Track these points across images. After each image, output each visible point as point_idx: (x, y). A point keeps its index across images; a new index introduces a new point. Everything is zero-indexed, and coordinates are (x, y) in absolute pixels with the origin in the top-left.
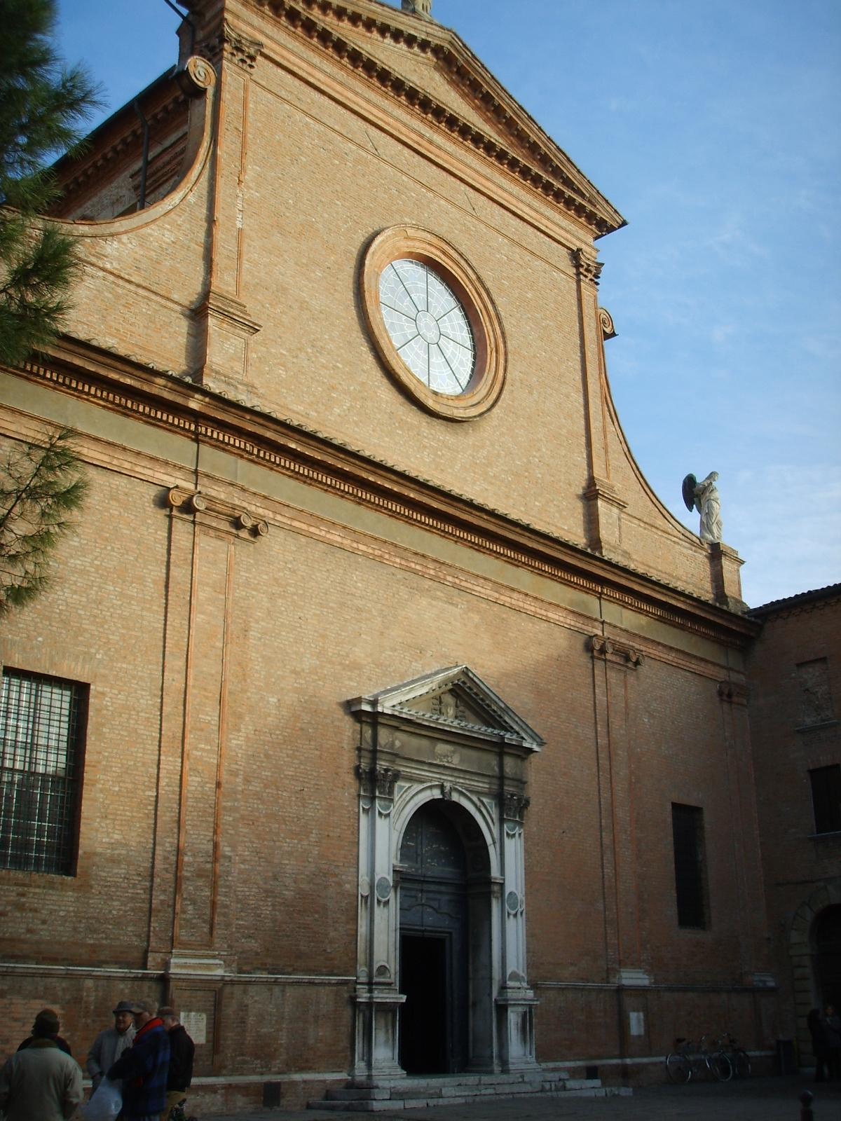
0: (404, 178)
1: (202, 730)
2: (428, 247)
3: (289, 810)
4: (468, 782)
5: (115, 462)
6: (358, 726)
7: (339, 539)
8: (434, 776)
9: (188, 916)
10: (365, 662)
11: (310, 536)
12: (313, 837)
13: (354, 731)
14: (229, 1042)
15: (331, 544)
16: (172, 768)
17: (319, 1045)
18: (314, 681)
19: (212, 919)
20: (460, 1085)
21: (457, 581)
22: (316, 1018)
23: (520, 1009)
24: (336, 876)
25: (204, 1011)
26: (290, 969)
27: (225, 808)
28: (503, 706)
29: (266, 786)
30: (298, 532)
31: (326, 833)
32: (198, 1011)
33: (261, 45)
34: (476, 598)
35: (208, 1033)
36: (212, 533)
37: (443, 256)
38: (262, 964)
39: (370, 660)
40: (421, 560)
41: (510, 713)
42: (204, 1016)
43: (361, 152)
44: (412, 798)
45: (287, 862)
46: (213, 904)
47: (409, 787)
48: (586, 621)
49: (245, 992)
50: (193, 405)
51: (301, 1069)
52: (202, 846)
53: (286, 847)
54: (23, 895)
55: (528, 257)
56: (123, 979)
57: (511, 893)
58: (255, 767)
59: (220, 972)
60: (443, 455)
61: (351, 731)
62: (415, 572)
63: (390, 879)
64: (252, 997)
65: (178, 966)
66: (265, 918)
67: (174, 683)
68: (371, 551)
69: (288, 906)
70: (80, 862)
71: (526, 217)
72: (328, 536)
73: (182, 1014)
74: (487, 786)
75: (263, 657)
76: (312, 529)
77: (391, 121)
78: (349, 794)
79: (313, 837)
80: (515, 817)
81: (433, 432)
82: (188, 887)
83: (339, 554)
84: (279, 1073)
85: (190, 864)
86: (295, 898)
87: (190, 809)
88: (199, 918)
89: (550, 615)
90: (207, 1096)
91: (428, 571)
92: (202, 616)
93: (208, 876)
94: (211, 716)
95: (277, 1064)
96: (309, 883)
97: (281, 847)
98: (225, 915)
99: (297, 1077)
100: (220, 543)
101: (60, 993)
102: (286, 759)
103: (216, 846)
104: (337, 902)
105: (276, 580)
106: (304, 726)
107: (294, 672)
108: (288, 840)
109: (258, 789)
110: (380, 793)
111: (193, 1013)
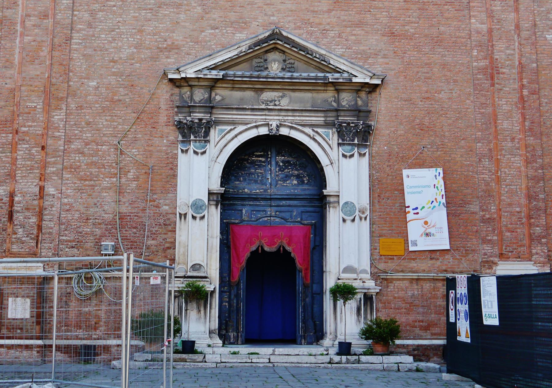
1: (30, 113)
4: (298, 118)
8: (259, 118)
9: (18, 236)
10: (185, 43)
12: (130, 175)
13: (172, 95)
16: (5, 141)
19: (38, 236)
25: (28, 297)
27: (49, 162)
29: (87, 144)
32: (23, 297)
42: (28, 301)
44: (236, 136)
46: (40, 228)
47: (231, 130)
52: (30, 190)
53: (105, 184)
57: (346, 203)
58: (76, 132)
67: (6, 86)
69: (107, 225)
73: (10, 299)
74: (323, 119)
75: (84, 55)
79: (130, 175)
80: (353, 140)
82: (19, 217)
85: (19, 203)
87: (19, 166)
88: (27, 237)
92: (29, 38)
94: (36, 103)
97: (101, 184)
102: (104, 123)
103: (42, 189)
106: (121, 98)
108: (107, 179)
109: (80, 147)
110: (195, 137)
111: (19, 299)
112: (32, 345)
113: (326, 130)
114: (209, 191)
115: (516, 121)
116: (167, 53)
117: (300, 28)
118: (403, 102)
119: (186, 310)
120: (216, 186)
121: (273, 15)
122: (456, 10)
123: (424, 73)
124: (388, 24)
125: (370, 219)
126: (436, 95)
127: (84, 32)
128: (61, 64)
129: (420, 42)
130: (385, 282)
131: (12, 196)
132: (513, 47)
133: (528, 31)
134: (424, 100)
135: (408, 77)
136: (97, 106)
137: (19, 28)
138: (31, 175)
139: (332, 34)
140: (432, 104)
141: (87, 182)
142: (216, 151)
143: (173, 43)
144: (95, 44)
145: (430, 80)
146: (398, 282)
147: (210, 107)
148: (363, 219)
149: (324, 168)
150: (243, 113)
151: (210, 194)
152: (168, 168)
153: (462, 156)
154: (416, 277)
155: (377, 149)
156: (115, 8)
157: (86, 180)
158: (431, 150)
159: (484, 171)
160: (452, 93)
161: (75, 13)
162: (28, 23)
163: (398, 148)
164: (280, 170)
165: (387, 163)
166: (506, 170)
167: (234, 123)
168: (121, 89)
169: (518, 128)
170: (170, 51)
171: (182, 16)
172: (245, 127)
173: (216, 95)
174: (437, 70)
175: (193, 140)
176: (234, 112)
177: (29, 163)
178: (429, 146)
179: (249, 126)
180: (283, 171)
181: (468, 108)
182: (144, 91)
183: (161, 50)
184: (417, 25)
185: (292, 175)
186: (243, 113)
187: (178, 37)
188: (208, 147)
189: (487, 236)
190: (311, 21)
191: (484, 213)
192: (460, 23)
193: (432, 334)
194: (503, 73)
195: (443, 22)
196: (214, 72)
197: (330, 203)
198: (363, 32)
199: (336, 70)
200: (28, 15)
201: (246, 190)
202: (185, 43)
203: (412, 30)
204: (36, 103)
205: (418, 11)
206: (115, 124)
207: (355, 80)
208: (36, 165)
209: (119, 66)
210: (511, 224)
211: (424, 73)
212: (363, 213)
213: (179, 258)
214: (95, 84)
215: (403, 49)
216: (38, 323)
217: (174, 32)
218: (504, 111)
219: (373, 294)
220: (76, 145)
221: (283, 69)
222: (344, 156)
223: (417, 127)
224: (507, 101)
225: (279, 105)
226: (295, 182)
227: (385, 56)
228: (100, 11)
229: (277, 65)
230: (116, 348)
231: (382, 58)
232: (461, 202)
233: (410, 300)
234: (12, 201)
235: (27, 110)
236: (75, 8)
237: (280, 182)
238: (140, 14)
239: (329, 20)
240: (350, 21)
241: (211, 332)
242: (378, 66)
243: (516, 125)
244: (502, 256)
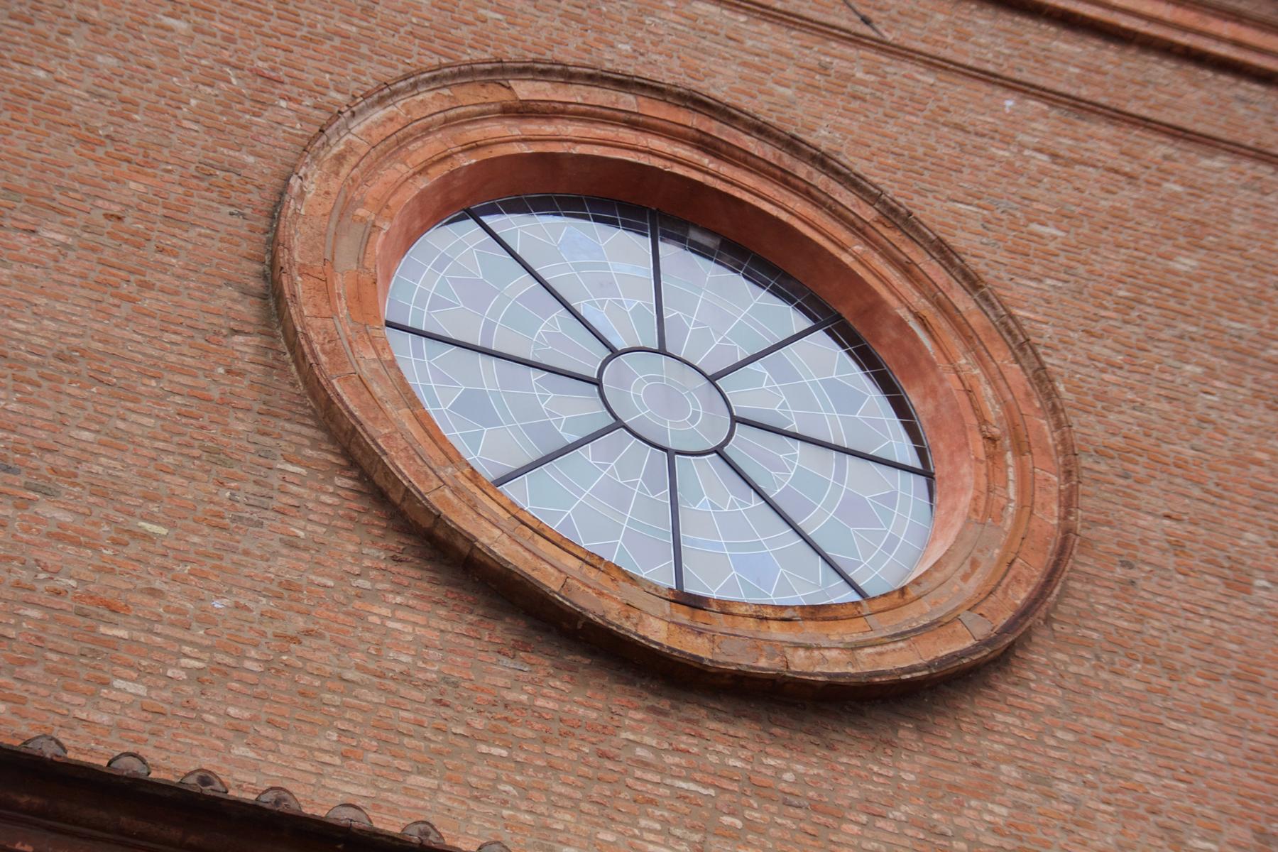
37: (706, 161)
55: (1159, 148)
60: (750, 825)
81: (684, 741)
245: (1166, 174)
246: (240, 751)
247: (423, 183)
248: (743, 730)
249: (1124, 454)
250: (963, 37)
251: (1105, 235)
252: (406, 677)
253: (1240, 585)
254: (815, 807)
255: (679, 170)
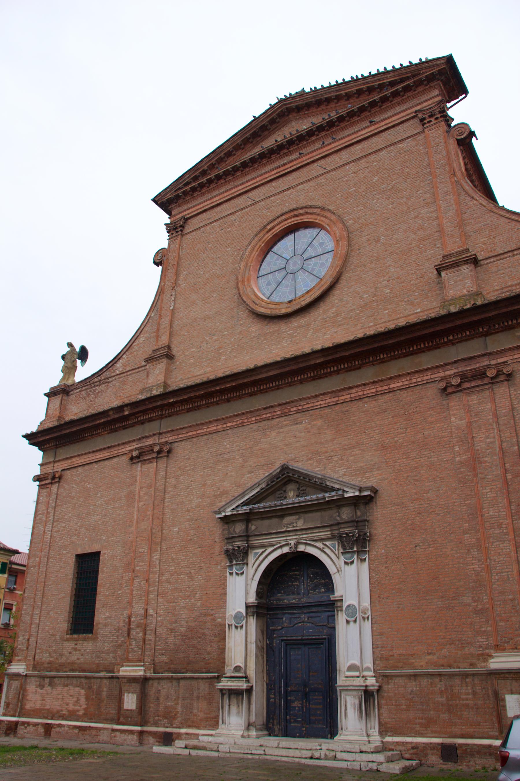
0: (272, 198)
2: (285, 223)
3: (184, 584)
4: (310, 535)
5: (112, 453)
6: (226, 527)
7: (215, 428)
8: (281, 539)
9: (133, 647)
10: (231, 488)
11: (197, 436)
12: (197, 596)
13: (223, 530)
14: (151, 709)
15: (210, 433)
17: (199, 713)
18: (199, 511)
20: (261, 746)
21: (300, 408)
22: (198, 697)
23: (355, 693)
24: (212, 615)
25: (135, 693)
26: (184, 670)
28: (320, 476)
30: (192, 437)
31: (205, 592)
32: (132, 693)
33: (183, 217)
34: (318, 410)
35: (137, 704)
36: (147, 462)
37: (296, 219)
38: (169, 668)
39: (234, 486)
40: (271, 410)
41: (328, 479)
42: (135, 696)
43: (243, 211)
44: (266, 557)
45: (182, 612)
46: (144, 641)
47: (263, 552)
48: (436, 371)
49: (159, 683)
50: (126, 413)
51: (189, 727)
52: (140, 612)
53: (182, 604)
54: (76, 644)
56: (106, 678)
57: (349, 606)
59: (141, 673)
60: (298, 333)
61: (221, 530)
62: (267, 419)
63: (243, 610)
64: (162, 686)
65: (123, 671)
66: (170, 644)
68: (235, 423)
69: (182, 636)
70: (95, 628)
71: (366, 136)
72: (208, 430)
73: (126, 694)
74: (329, 533)
76: (198, 432)
77: (258, 179)
78: (221, 567)
79: (197, 596)
80: (353, 548)
82: (133, 633)
83: (214, 436)
84: (176, 728)
85: (134, 621)
86: (186, 631)
89: (392, 386)
90: (129, 736)
91: (276, 414)
92: (142, 503)
93: (142, 627)
95: (176, 722)
96: (195, 621)
98: (150, 644)
99: (183, 731)
100: (151, 464)
101: (84, 685)
103: (146, 610)
104: (212, 630)
105: (179, 468)
106: (192, 537)
107: (188, 511)
110: (236, 561)
111: (130, 694)
112: (134, 730)
113: (333, 542)
114: (246, 604)
115: (502, 506)
116: (220, 499)
117: (310, 459)
118: (397, 507)
119: (229, 705)
120: (252, 599)
121: (291, 453)
122: (438, 413)
123: (413, 476)
124: (381, 440)
125: (371, 619)
126: (425, 495)
127: (172, 493)
128: (158, 518)
129: (408, 450)
130: (386, 679)
131: (130, 617)
132: (492, 435)
133: (506, 416)
134: (414, 502)
135: (399, 483)
136: (178, 545)
137: (137, 497)
138: (141, 601)
139: (335, 459)
140: (421, 504)
141: (172, 604)
142: (251, 571)
143: (224, 490)
144: (178, 500)
145: (418, 482)
146: (398, 679)
147: (247, 537)
148: (366, 620)
149: (333, 576)
150: (270, 537)
151: (247, 607)
152: (221, 588)
153: (452, 550)
154: (413, 674)
155: (375, 553)
156: (190, 471)
157: (171, 603)
158: (423, 547)
159: (474, 562)
160: (439, 490)
161: (168, 480)
162: (142, 493)
163: (394, 550)
164: (310, 581)
165: (385, 565)
166: (496, 558)
167: (265, 546)
168: (192, 531)
169: (504, 513)
170: (222, 497)
171: (230, 468)
172: (272, 549)
173: (252, 525)
174: (424, 471)
175: (235, 564)
176: (264, 537)
177: (139, 592)
178: (421, 544)
179: (275, 547)
180: (313, 581)
181: (455, 502)
182: (206, 530)
183: (216, 496)
184: (404, 435)
185: (321, 584)
186: (270, 537)
187: (227, 484)
188: (245, 568)
189: (481, 627)
190: (320, 450)
191: (476, 604)
192: (442, 424)
193: (432, 732)
194: (485, 462)
195: (427, 427)
196: (245, 508)
197: (337, 607)
198: (360, 451)
199: (333, 489)
200: (141, 488)
201: (285, 601)
202: (231, 488)
203: (400, 441)
204: (144, 548)
205: (405, 423)
206: (188, 557)
207: (346, 495)
208: (143, 594)
209: (191, 514)
210: (505, 613)
211: (413, 476)
212: (365, 613)
213: (228, 661)
214: (177, 529)
215: (394, 459)
216: (140, 714)
217: (224, 482)
218: (489, 499)
219: (374, 691)
220: (166, 576)
221: (298, 496)
222: (346, 563)
223: (409, 527)
224: (491, 489)
225: (296, 526)
226: (323, 590)
227: (379, 469)
228: (181, 475)
229: (292, 493)
230: (185, 736)
231: (377, 470)
232: (454, 595)
233: (409, 697)
234: (130, 621)
235: (139, 554)
236: (167, 477)
237: (311, 591)
238: (204, 472)
239: (333, 447)
240: (349, 445)
241: (249, 726)
242: (374, 478)
243: (502, 510)
244: (499, 648)
245: (373, 161)
246: (235, 359)
247: (257, 253)
248: (298, 318)
249: (361, 228)
250: (341, 159)
251: (362, 183)
252: (254, 337)
253: (378, 241)
254: (307, 325)
255: (292, 223)
